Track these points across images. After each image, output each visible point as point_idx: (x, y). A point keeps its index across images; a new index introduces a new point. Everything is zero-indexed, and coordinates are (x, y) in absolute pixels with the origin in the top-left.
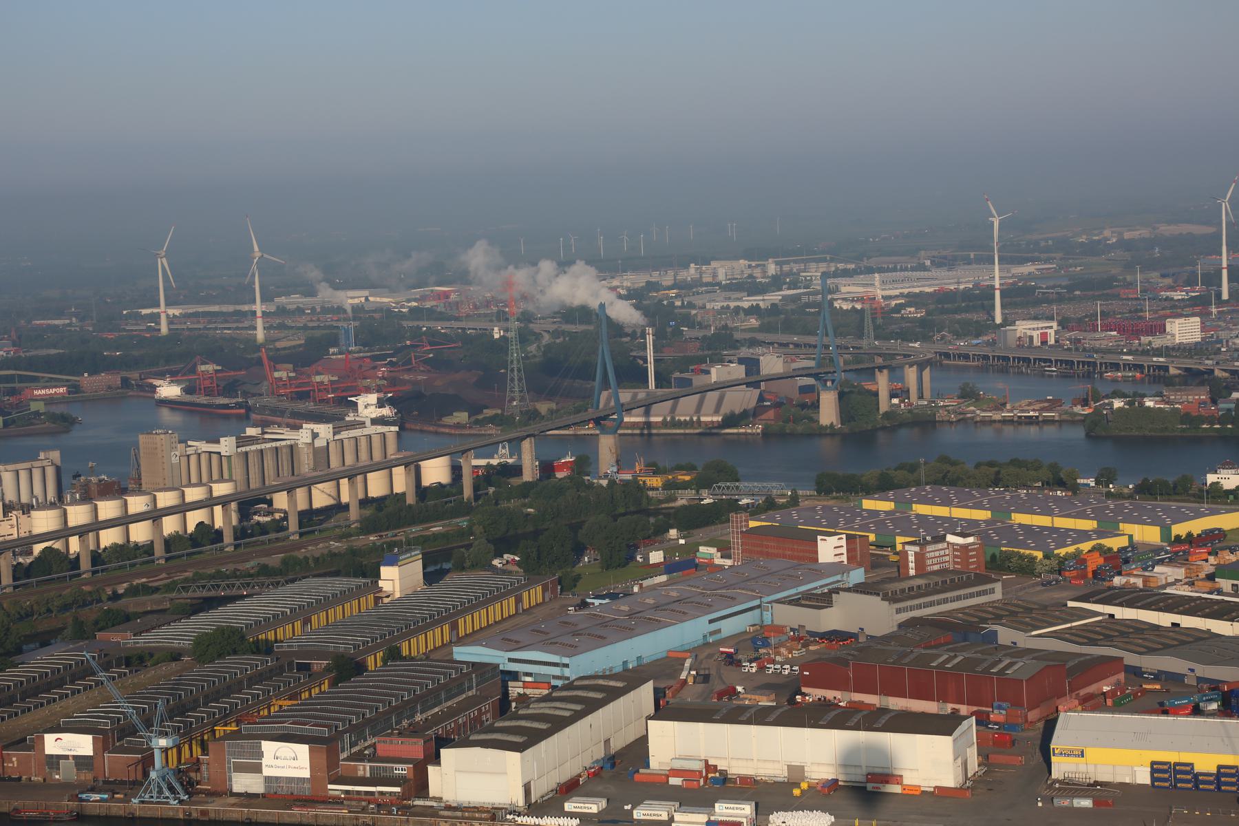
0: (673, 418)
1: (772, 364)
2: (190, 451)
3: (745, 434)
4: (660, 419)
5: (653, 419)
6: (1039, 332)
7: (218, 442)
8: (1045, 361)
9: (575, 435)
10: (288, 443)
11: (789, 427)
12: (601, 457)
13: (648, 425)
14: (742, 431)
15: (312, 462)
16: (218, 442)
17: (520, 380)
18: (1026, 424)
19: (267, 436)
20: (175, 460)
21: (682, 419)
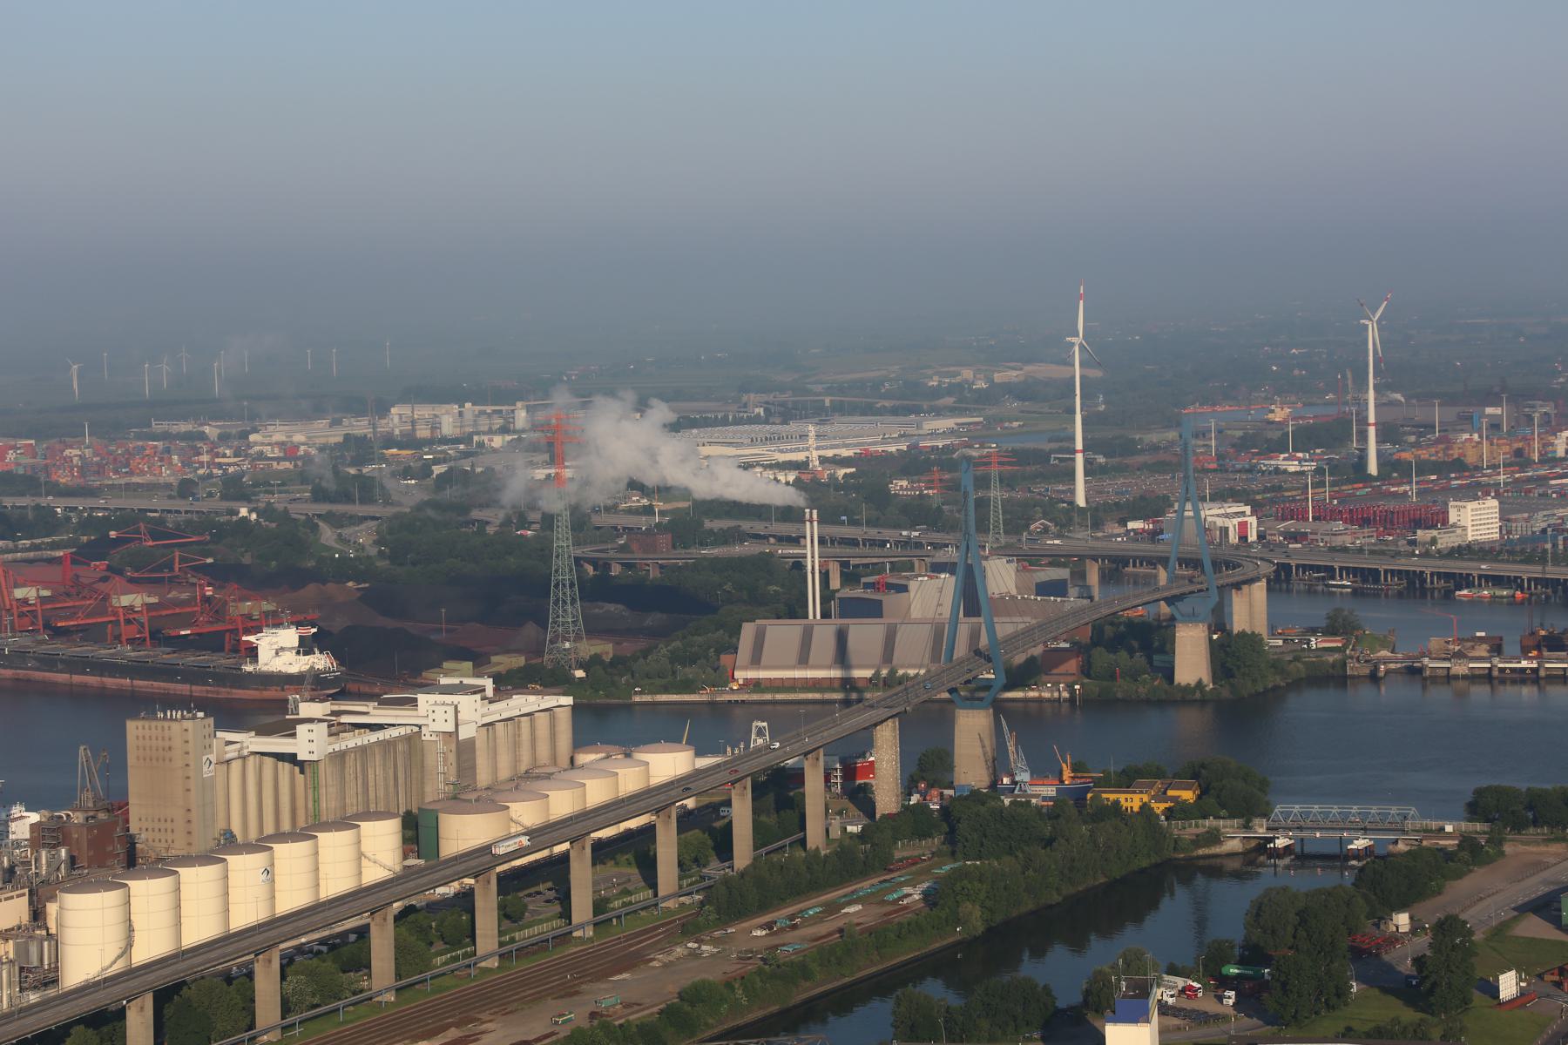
0: (893, 672)
1: (1001, 577)
2: (231, 751)
3: (1040, 700)
4: (868, 673)
5: (858, 673)
6: (1236, 521)
7: (293, 735)
8: (1318, 569)
9: (712, 704)
10: (402, 731)
11: (1122, 688)
12: (957, 751)
13: (847, 684)
14: (1032, 694)
15: (453, 770)
16: (293, 735)
17: (573, 601)
18: (1514, 682)
19: (345, 719)
20: (207, 771)
21: (912, 672)
